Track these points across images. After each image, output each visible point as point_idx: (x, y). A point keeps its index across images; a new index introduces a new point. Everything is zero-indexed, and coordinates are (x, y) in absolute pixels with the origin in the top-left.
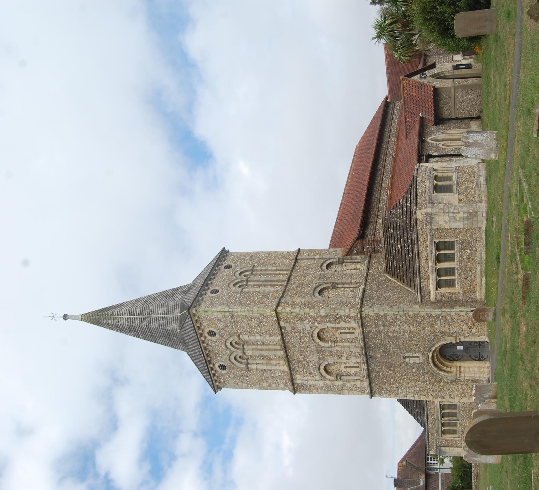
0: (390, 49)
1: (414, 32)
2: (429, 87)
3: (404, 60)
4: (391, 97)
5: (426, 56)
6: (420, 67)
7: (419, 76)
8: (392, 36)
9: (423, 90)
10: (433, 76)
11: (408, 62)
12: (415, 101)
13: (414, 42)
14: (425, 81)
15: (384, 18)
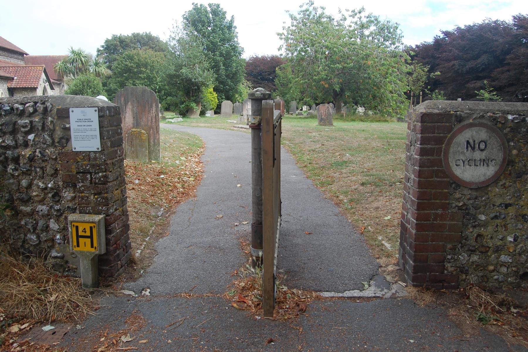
0: (66, 60)
1: (76, 76)
2: (36, 85)
3: (56, 68)
4: (27, 58)
5: (59, 84)
6: (52, 81)
7: (45, 78)
8: (73, 61)
9: (35, 80)
10: (45, 88)
11: (55, 71)
12: (26, 74)
13: (69, 75)
14: (41, 82)
15: (85, 57)
